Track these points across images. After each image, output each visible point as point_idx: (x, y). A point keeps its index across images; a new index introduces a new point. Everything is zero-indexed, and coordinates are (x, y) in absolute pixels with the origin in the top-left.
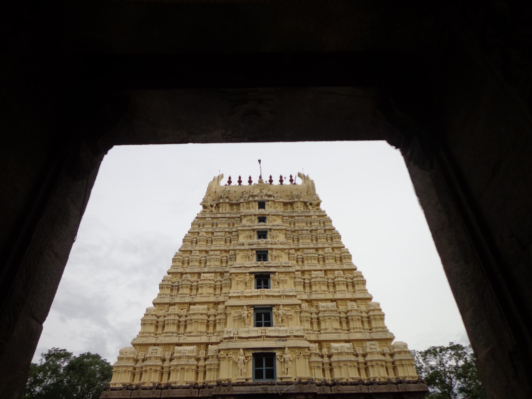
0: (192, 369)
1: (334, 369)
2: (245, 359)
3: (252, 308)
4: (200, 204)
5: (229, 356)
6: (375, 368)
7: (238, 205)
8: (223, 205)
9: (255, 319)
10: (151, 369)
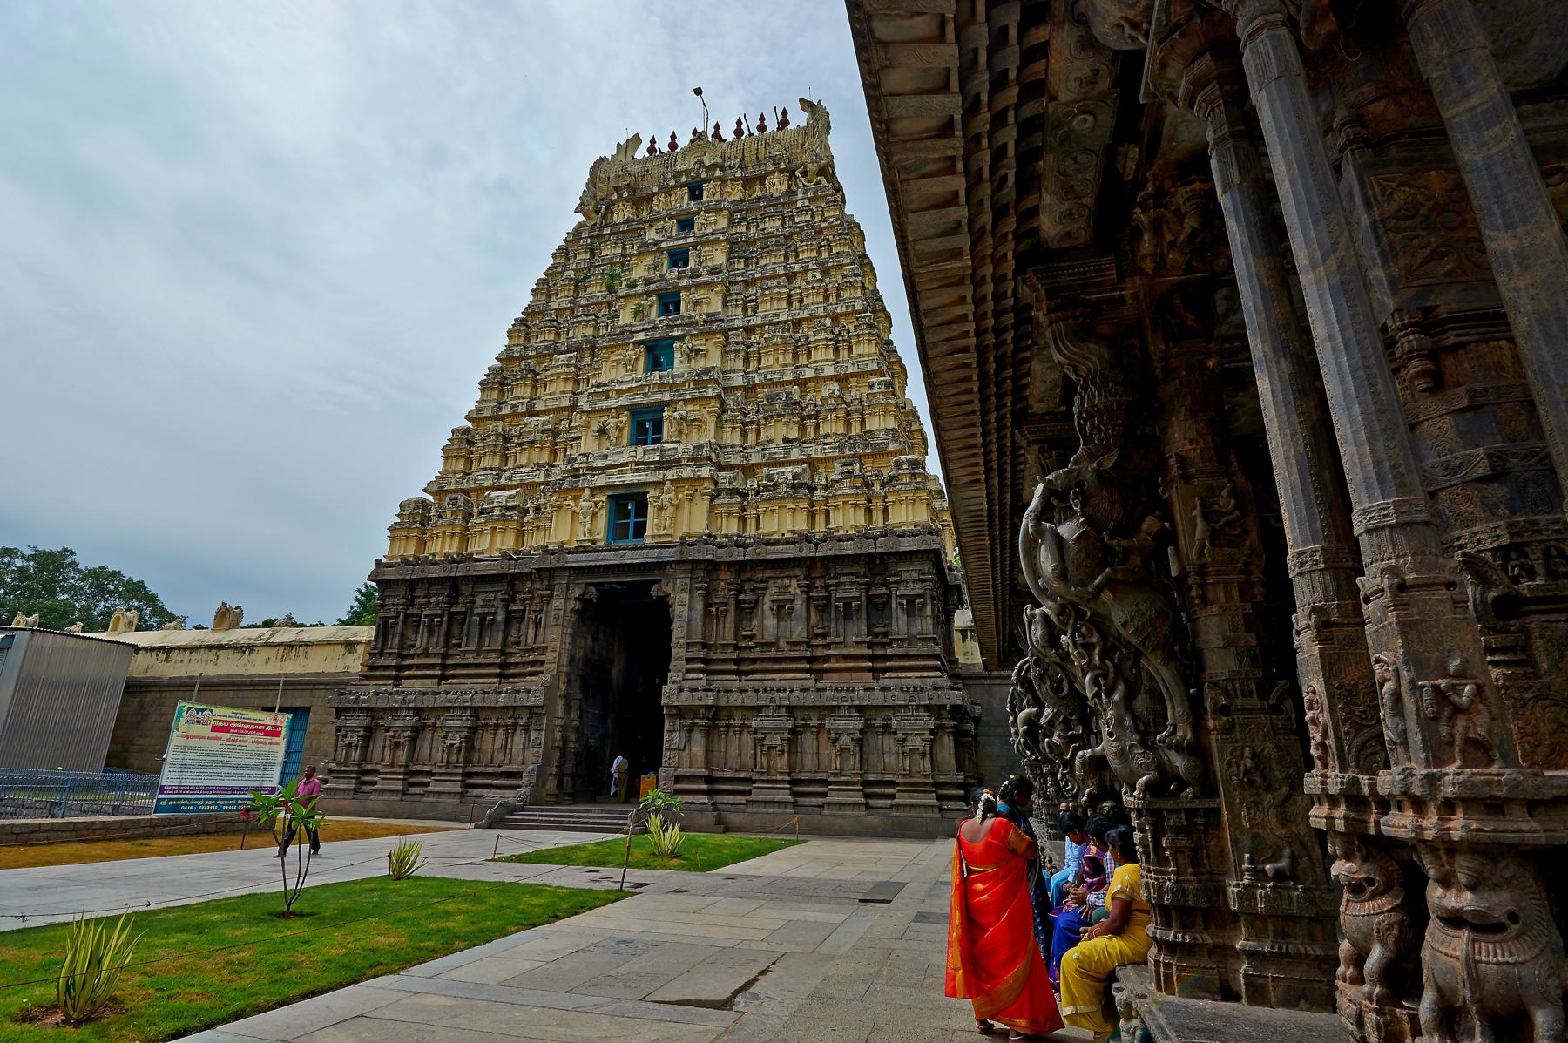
7: (649, 199)
9: (634, 432)
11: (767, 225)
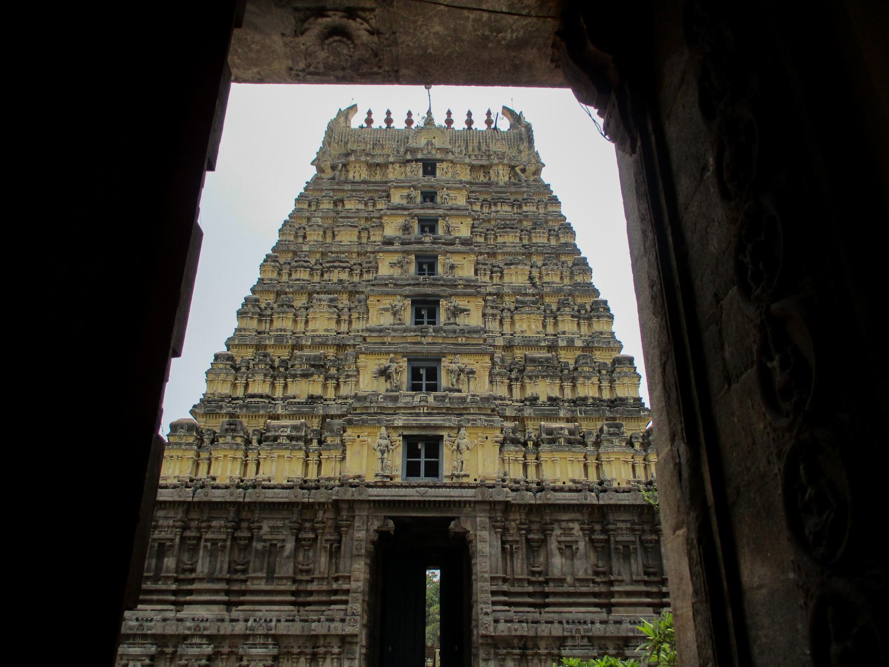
0: (298, 458)
1: (544, 465)
2: (389, 444)
3: (405, 359)
4: (312, 164)
5: (361, 438)
6: (613, 466)
8: (355, 167)
9: (410, 377)
10: (225, 456)
11: (499, 208)
